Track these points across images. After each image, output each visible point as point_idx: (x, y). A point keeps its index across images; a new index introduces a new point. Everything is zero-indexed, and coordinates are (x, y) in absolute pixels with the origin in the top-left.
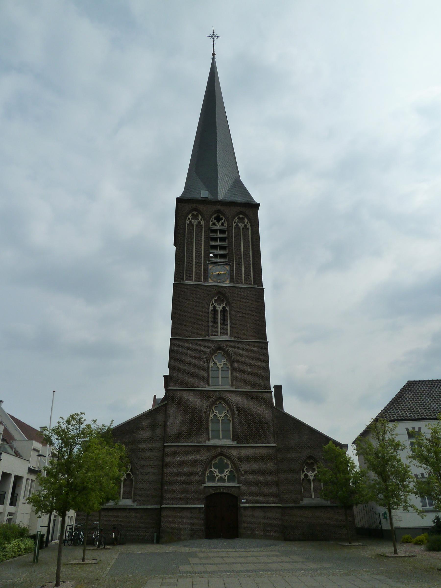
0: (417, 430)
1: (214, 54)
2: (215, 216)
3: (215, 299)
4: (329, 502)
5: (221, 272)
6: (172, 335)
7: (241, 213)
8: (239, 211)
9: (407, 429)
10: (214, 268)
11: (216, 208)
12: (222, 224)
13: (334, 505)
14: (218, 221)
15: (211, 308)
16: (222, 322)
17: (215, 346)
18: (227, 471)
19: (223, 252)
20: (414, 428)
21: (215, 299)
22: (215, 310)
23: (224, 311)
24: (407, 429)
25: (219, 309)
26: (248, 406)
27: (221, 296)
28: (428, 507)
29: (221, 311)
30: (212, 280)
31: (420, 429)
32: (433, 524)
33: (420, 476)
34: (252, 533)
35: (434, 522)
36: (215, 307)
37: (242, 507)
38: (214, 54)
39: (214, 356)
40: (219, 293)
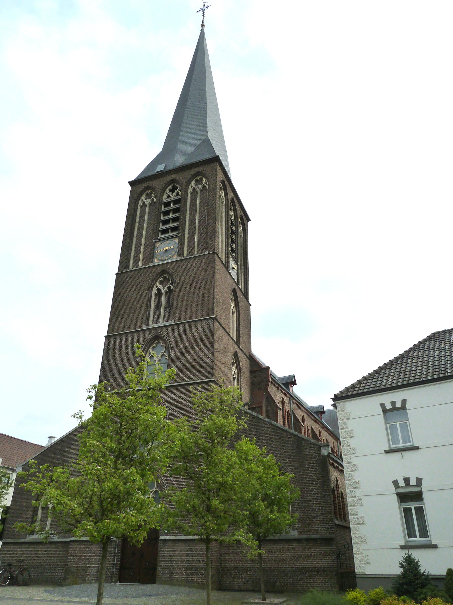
0: (399, 405)
1: (203, 26)
2: (170, 187)
3: (159, 280)
4: (296, 532)
5: (167, 248)
6: (108, 332)
7: (198, 174)
8: (195, 173)
9: (383, 405)
10: (162, 245)
11: (169, 178)
12: (178, 194)
13: (304, 537)
14: (173, 192)
15: (155, 291)
16: (167, 305)
17: (151, 335)
18: (151, 492)
19: (175, 224)
20: (394, 403)
21: (159, 280)
22: (159, 294)
23: (169, 292)
24: (383, 405)
25: (164, 290)
26: (182, 404)
27: (166, 275)
28: (418, 538)
29: (166, 293)
30: (158, 260)
31: (404, 402)
32: (402, 570)
33: (402, 483)
34: (169, 577)
35: (402, 566)
36: (159, 290)
37: (161, 540)
38: (203, 26)
39: (151, 348)
40: (163, 272)
